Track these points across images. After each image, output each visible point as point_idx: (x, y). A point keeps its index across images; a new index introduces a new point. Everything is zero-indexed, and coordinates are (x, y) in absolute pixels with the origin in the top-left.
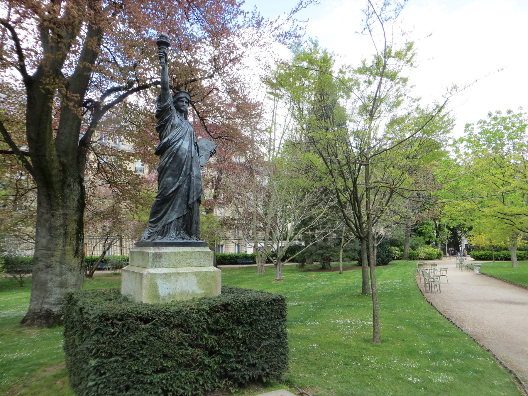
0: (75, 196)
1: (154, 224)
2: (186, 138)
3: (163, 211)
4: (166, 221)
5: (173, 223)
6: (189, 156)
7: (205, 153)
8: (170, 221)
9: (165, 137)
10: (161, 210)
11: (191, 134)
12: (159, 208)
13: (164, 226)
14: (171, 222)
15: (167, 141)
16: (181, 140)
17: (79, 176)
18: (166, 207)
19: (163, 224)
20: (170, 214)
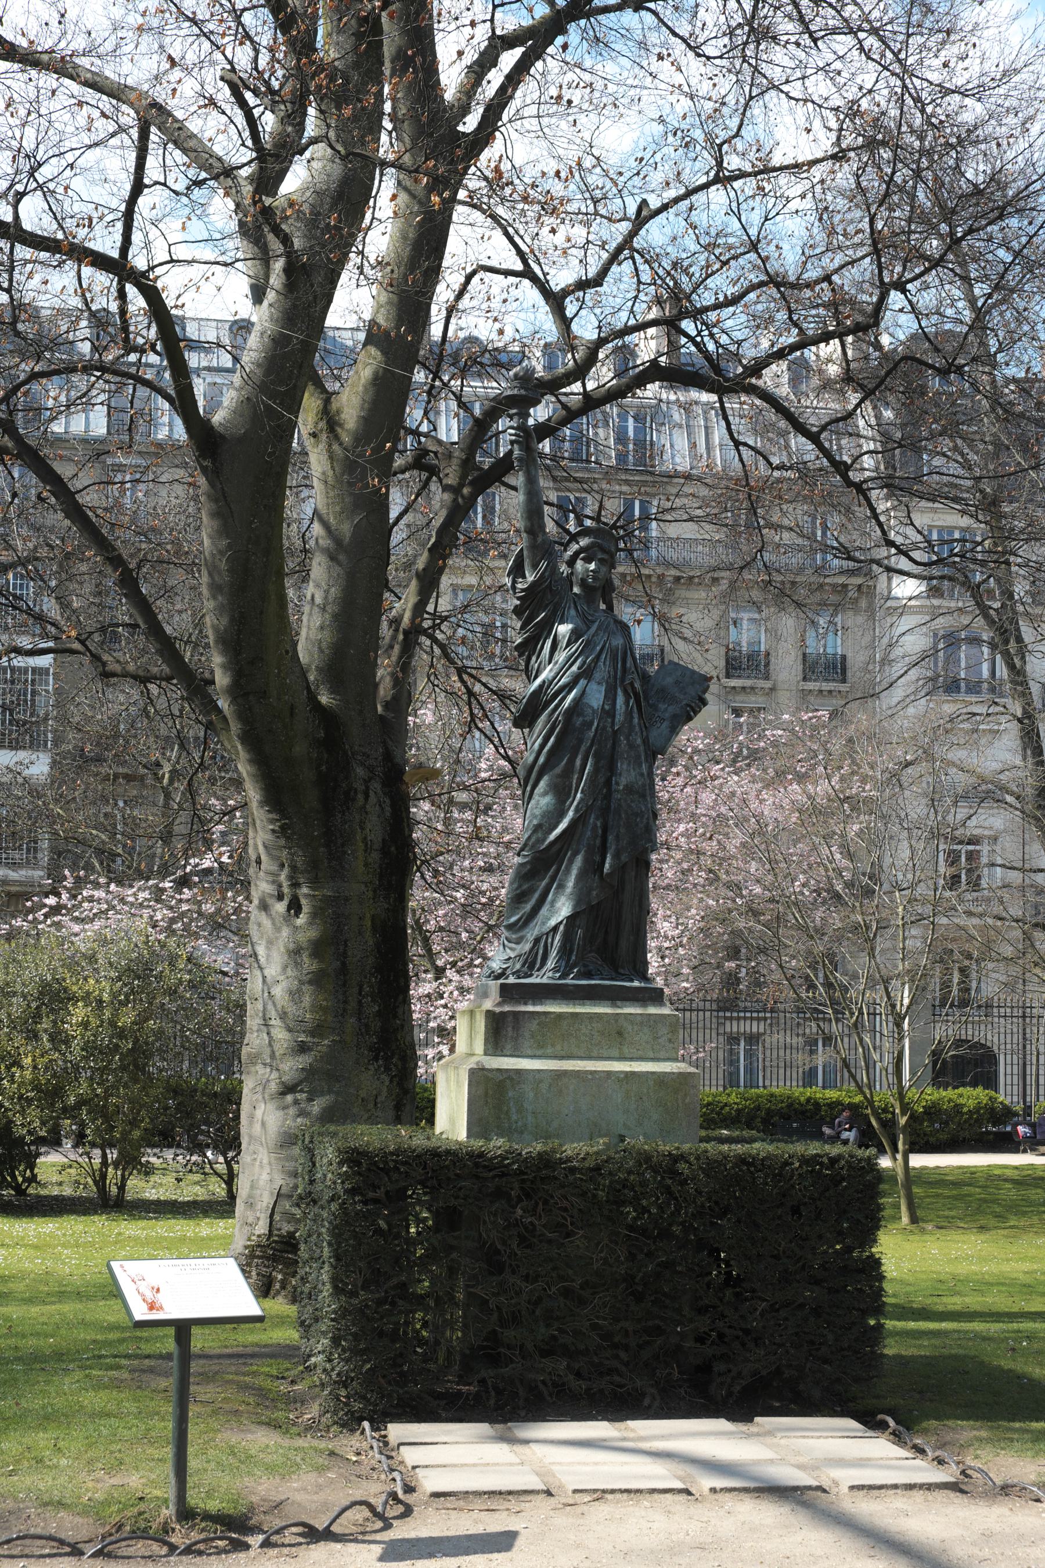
0: (374, 829)
1: (515, 932)
2: (597, 675)
3: (536, 895)
4: (544, 924)
5: (562, 928)
6: (604, 728)
7: (671, 709)
8: (553, 922)
9: (536, 677)
10: (531, 891)
11: (614, 659)
12: (525, 887)
13: (537, 941)
14: (555, 929)
15: (541, 686)
16: (582, 682)
17: (388, 756)
18: (544, 883)
19: (536, 932)
20: (553, 902)
